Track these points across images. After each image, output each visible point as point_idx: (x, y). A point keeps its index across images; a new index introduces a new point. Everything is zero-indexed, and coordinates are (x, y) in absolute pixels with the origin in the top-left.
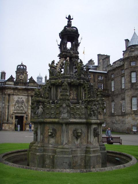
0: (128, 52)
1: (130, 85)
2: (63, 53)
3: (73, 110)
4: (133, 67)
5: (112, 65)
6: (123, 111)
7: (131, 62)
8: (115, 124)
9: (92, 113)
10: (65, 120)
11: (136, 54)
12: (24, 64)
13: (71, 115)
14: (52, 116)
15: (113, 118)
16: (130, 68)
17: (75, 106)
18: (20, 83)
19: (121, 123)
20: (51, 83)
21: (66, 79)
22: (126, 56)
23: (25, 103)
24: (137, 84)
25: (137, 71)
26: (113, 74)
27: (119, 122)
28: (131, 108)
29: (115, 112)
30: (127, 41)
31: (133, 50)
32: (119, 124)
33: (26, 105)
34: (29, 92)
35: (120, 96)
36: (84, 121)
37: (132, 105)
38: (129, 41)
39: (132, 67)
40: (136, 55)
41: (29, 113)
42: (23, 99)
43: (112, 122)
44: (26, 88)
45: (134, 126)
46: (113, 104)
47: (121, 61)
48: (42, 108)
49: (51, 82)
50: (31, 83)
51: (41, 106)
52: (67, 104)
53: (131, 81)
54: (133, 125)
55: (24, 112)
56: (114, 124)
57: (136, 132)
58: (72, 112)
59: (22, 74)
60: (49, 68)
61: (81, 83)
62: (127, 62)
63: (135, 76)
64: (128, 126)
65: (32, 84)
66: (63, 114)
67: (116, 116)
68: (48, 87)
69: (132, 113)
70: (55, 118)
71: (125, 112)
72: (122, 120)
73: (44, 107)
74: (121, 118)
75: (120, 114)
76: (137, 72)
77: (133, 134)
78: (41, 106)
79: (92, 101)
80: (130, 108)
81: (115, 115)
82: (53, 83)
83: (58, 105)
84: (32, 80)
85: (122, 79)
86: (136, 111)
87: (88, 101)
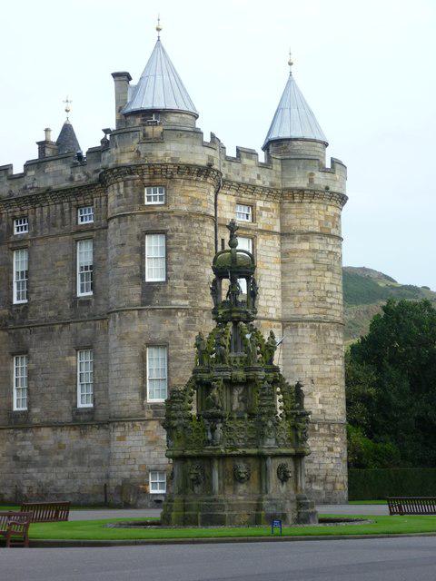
0: (136, 141)
1: (137, 289)
5: (18, 169)
6: (80, 405)
8: (35, 465)
11: (172, 156)
15: (23, 439)
19: (70, 462)
24: (168, 292)
26: (23, 218)
27: (61, 457)
28: (143, 394)
29: (35, 411)
30: (122, 78)
32: (59, 464)
35: (66, 332)
36: (292, 451)
37: (144, 381)
39: (150, 212)
43: (16, 458)
45: (154, 471)
46: (18, 369)
53: (143, 277)
54: (153, 467)
56: (26, 467)
57: (163, 498)
62: (125, 186)
63: (161, 254)
64: (126, 474)
67: (38, 427)
69: (148, 415)
70: (246, 447)
71: (91, 412)
72: (76, 447)
74: (69, 437)
75: (67, 417)
76: (172, 237)
77: (152, 507)
80: (136, 396)
81: (35, 420)
85: (75, 252)
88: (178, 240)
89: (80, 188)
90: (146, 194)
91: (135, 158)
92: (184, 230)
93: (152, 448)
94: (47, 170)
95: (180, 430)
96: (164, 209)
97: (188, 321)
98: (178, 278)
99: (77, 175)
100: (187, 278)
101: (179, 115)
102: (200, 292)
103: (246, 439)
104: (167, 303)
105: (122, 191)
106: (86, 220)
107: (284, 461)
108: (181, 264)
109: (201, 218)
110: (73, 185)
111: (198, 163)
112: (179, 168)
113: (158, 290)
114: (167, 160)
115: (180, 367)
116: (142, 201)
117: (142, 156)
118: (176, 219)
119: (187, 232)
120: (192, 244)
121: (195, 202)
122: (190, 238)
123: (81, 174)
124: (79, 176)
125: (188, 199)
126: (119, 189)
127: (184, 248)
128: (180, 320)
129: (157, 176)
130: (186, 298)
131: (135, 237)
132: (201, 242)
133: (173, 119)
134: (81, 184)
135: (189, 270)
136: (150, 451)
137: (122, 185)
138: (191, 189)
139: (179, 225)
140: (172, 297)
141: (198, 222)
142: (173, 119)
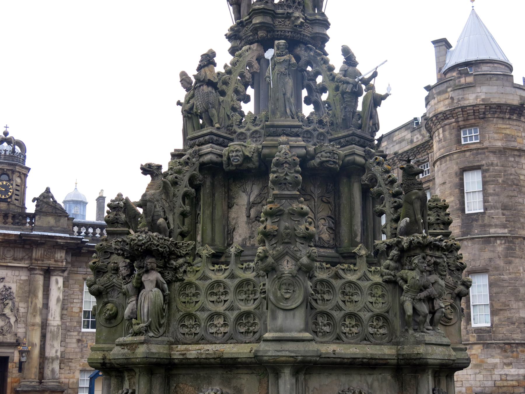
2: (257, 20)
3: (326, 297)
4: (470, 150)
7: (460, 128)
9: (424, 308)
11: (483, 97)
13: (320, 320)
14: (213, 330)
16: (455, 156)
17: (337, 276)
20: (202, 160)
22: (442, 108)
23: (17, 300)
24: (486, 222)
25: (485, 168)
31: (470, 79)
33: (22, 310)
34: (37, 253)
38: (448, 46)
40: (483, 100)
41: (33, 345)
42: (8, 285)
44: (20, 236)
47: (414, 130)
48: (158, 285)
49: (201, 156)
50: (46, 214)
51: (155, 276)
53: (463, 210)
55: (9, 338)
58: (320, 307)
60: (182, 94)
61: (354, 163)
65: (51, 220)
66: (281, 315)
68: (186, 178)
70: (229, 339)
73: (169, 283)
76: (487, 171)
78: (155, 276)
79: (422, 246)
82: (214, 158)
83: (246, 269)
84: (48, 203)
86: (489, 332)
87: (402, 251)
88: (494, 173)
89: (417, 147)
90: (462, 136)
91: (449, 104)
92: (499, 164)
93: (477, 371)
94: (395, 139)
95: (115, 297)
96: (479, 146)
97: (508, 249)
98: (494, 207)
99: (415, 137)
100: (505, 208)
101: (491, 65)
102: (519, 220)
103: (232, 316)
104: (485, 232)
105: (441, 136)
106: (428, 173)
108: (498, 195)
109: (516, 153)
110: (414, 145)
111: (509, 102)
112: (491, 108)
113: (477, 220)
114: (479, 101)
115: (502, 292)
116: (459, 141)
117: (455, 101)
118: (491, 155)
119: (502, 166)
120: (506, 177)
121: (508, 138)
122: (505, 171)
123: (418, 136)
124: (417, 138)
125: (501, 136)
126: (439, 135)
127: (500, 180)
128: (500, 247)
129: (470, 117)
130: (504, 227)
131: (454, 175)
132: (518, 175)
133: (485, 69)
134: (419, 143)
135: (506, 200)
136: (476, 374)
137: (441, 130)
138: (505, 126)
139: (493, 159)
140: (490, 226)
141: (514, 156)
142: (485, 69)
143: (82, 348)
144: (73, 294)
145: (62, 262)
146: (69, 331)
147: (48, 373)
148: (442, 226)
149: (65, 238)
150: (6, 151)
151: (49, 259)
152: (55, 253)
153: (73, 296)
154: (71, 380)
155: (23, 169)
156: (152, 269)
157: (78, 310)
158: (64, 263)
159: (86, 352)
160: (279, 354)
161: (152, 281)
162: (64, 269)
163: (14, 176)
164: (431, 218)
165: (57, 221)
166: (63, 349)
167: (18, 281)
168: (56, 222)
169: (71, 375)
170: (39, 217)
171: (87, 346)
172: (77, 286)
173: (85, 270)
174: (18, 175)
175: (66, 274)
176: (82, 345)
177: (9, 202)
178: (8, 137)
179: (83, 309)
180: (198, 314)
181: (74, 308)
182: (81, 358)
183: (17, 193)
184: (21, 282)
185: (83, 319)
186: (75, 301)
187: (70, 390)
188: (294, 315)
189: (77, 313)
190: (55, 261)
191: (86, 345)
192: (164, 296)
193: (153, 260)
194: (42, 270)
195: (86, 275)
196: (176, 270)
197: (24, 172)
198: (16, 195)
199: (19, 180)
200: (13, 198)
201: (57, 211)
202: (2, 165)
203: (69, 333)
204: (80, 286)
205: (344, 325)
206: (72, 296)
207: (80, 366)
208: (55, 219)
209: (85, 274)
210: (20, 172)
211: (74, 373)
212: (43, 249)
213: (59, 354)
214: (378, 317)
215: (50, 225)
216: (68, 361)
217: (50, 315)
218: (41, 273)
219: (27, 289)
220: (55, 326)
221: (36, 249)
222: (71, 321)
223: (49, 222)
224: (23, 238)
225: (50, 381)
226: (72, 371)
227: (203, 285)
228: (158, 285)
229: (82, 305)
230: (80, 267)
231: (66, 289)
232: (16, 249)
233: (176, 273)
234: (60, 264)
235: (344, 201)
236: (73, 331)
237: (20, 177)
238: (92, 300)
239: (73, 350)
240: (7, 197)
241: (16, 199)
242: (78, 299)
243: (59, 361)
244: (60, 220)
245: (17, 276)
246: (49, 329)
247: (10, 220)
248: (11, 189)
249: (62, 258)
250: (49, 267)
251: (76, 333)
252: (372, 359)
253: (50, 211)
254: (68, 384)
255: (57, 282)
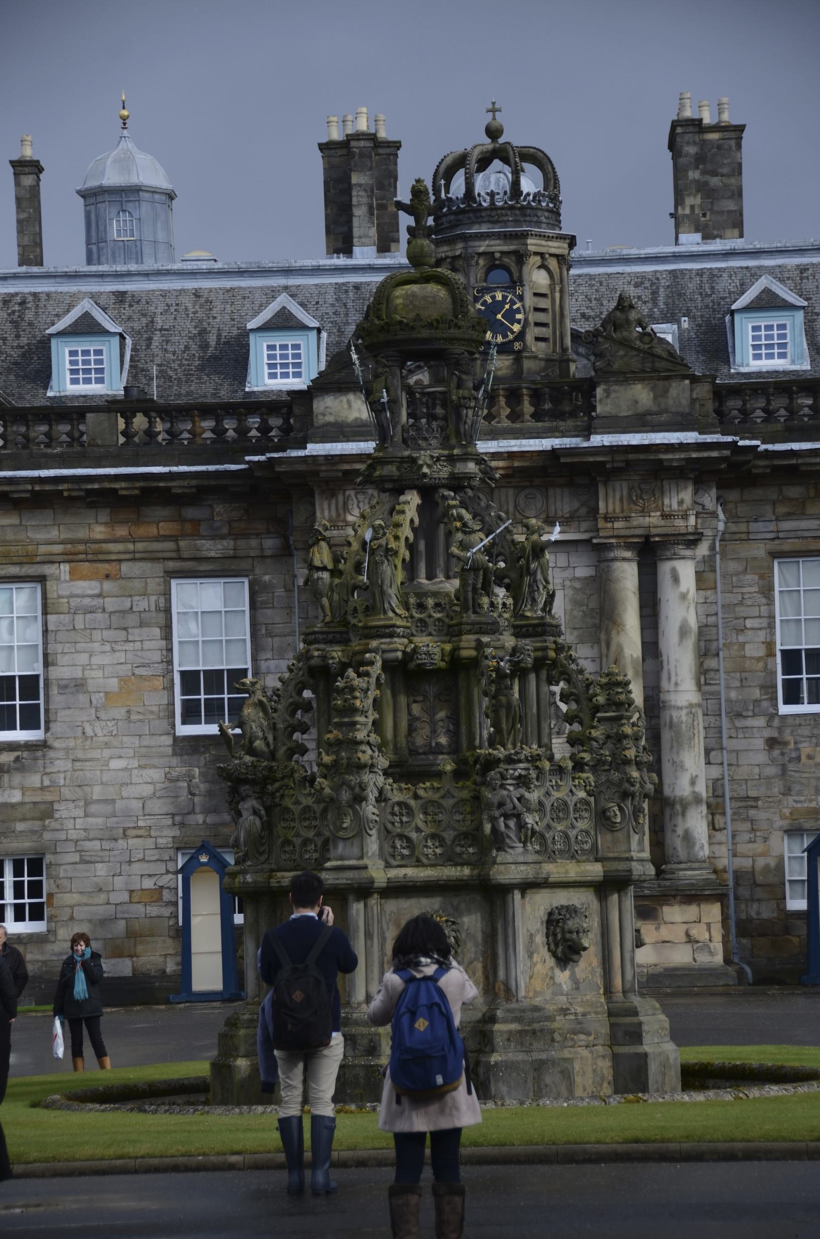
10: (350, 874)
12: (514, 137)
14: (307, 857)
18: (491, 398)
21: (374, 644)
44: (554, 453)
50: (626, 377)
52: (357, 790)
59: (500, 276)
84: (625, 344)
107: (562, 898)
143: (784, 765)
144: (741, 603)
145: (685, 517)
146: (739, 715)
147: (675, 843)
148: (614, 708)
149: (682, 447)
150: (492, 195)
151: (644, 512)
152: (663, 494)
153: (741, 611)
154: (761, 862)
155: (550, 243)
156: (248, 796)
157: (761, 652)
158: (692, 520)
159: (797, 775)
160: (337, 882)
161: (247, 810)
162: (691, 538)
163: (526, 269)
164: (599, 698)
165: (660, 395)
166: (715, 772)
167: (568, 583)
168: (655, 398)
169: (759, 847)
170: (605, 390)
171: (799, 759)
172: (750, 578)
173: (772, 526)
174: (539, 264)
175: (703, 549)
176: (783, 754)
177: (519, 352)
178: (501, 140)
179: (779, 647)
180: (294, 839)
181: (747, 646)
182: (784, 794)
183: (541, 317)
184: (578, 585)
185: (780, 677)
186: (749, 623)
187: (758, 889)
188: (352, 843)
189: (759, 659)
190: (664, 516)
191: (794, 755)
192: (262, 823)
193: (247, 787)
194: (628, 546)
195: (777, 542)
196: (273, 794)
197: (553, 251)
198: (537, 324)
199: (540, 279)
200: (529, 338)
201: (657, 365)
202: (487, 243)
203: (739, 723)
204: (762, 577)
205: (426, 846)
206: (738, 609)
207: (782, 817)
208: (653, 389)
209: (773, 539)
210: (542, 255)
211: (766, 839)
212: (625, 485)
213: (701, 788)
214: (465, 835)
215: (641, 409)
216: (743, 804)
217: (664, 675)
218: (628, 554)
219: (593, 604)
220: (681, 708)
221: (606, 485)
222: (742, 686)
223: (636, 402)
224: (562, 460)
225: (683, 866)
226: (758, 834)
227: (296, 809)
228: (255, 812)
229: (773, 634)
230: (756, 521)
231: (709, 593)
232: (551, 492)
233: (274, 798)
234: (679, 523)
235: (463, 699)
236: (750, 714)
237: (543, 266)
238: (803, 617)
239: (757, 770)
240: (511, 337)
241: (538, 339)
242: (760, 617)
243: (704, 809)
244: (667, 391)
245: (564, 569)
246: (665, 716)
247: (528, 408)
248: (518, 311)
249: (685, 507)
250: (647, 537)
251: (761, 722)
252: (448, 880)
253: (635, 363)
254: (753, 872)
255: (676, 579)
